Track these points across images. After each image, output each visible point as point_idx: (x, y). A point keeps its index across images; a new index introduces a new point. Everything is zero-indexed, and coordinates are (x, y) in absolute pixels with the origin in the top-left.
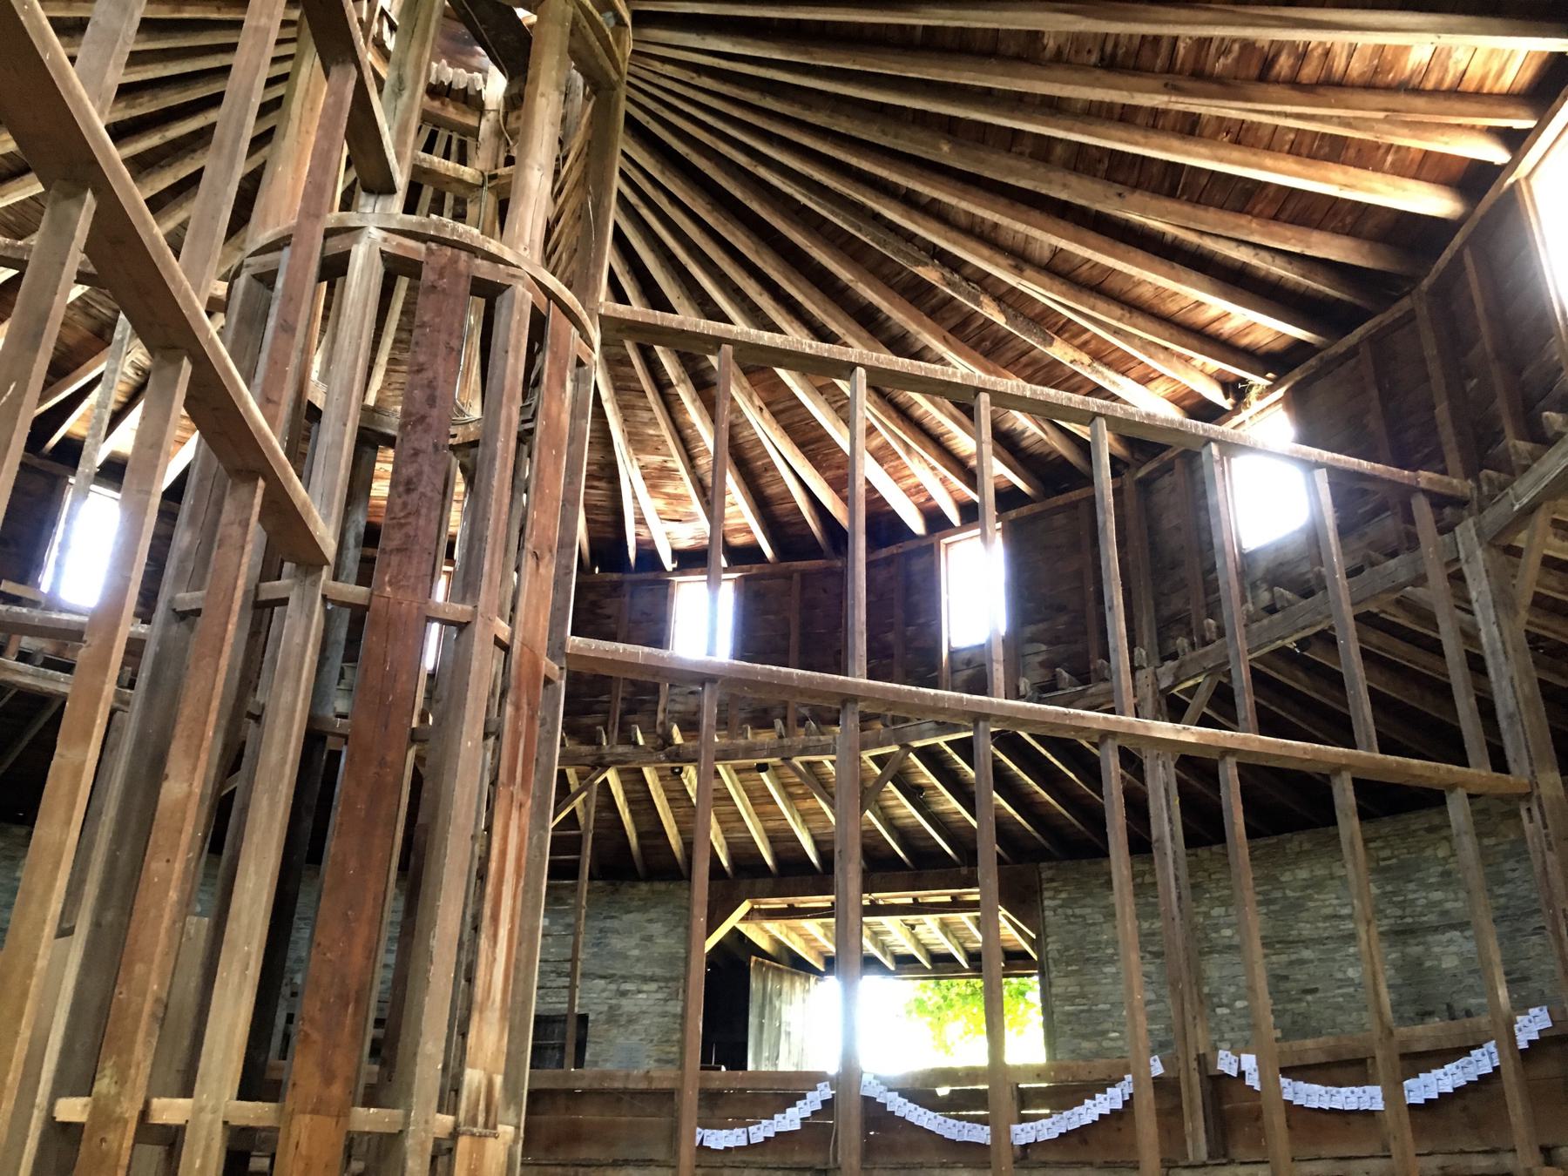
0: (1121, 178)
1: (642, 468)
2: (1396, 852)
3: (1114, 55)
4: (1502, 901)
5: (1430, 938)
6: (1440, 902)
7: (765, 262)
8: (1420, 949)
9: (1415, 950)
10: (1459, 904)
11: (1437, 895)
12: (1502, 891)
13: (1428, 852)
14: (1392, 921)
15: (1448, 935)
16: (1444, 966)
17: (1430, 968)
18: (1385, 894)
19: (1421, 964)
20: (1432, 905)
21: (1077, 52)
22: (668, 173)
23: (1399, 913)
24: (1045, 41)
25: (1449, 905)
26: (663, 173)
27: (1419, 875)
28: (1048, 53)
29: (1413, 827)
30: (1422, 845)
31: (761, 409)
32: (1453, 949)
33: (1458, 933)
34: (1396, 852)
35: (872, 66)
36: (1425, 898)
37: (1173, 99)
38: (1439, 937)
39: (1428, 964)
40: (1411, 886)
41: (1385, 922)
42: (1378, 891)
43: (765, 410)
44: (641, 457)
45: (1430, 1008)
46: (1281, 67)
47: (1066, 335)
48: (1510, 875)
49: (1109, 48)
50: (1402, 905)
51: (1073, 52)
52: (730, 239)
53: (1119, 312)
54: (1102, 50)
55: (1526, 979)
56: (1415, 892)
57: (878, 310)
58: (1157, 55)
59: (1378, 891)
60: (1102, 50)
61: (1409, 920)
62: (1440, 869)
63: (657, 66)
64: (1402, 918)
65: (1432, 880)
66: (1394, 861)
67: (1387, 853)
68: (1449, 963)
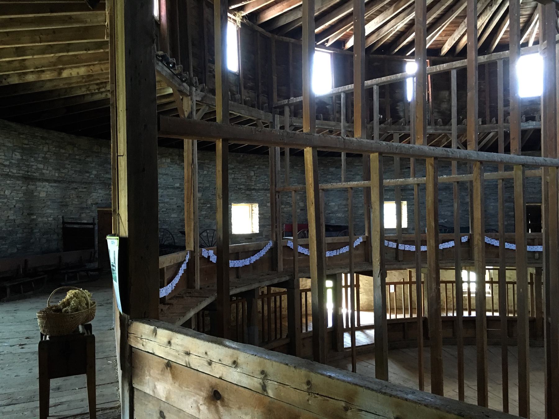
2: (30, 143)
4: (63, 175)
5: (38, 184)
6: (41, 169)
8: (33, 187)
9: (31, 187)
10: (48, 172)
11: (41, 166)
12: (64, 171)
13: (41, 147)
14: (23, 172)
15: (44, 183)
16: (41, 196)
17: (36, 196)
18: (22, 159)
19: (33, 193)
20: (38, 169)
23: (27, 169)
25: (44, 171)
27: (36, 155)
29: (37, 134)
30: (39, 143)
32: (44, 189)
33: (47, 184)
34: (30, 143)
36: (37, 166)
38: (41, 184)
39: (35, 194)
40: (32, 159)
41: (21, 172)
42: (20, 158)
45: (32, 212)
48: (67, 166)
50: (28, 166)
55: (67, 205)
56: (32, 162)
59: (20, 158)
61: (29, 174)
62: (44, 155)
64: (28, 172)
65: (40, 159)
66: (28, 146)
67: (26, 142)
68: (43, 195)
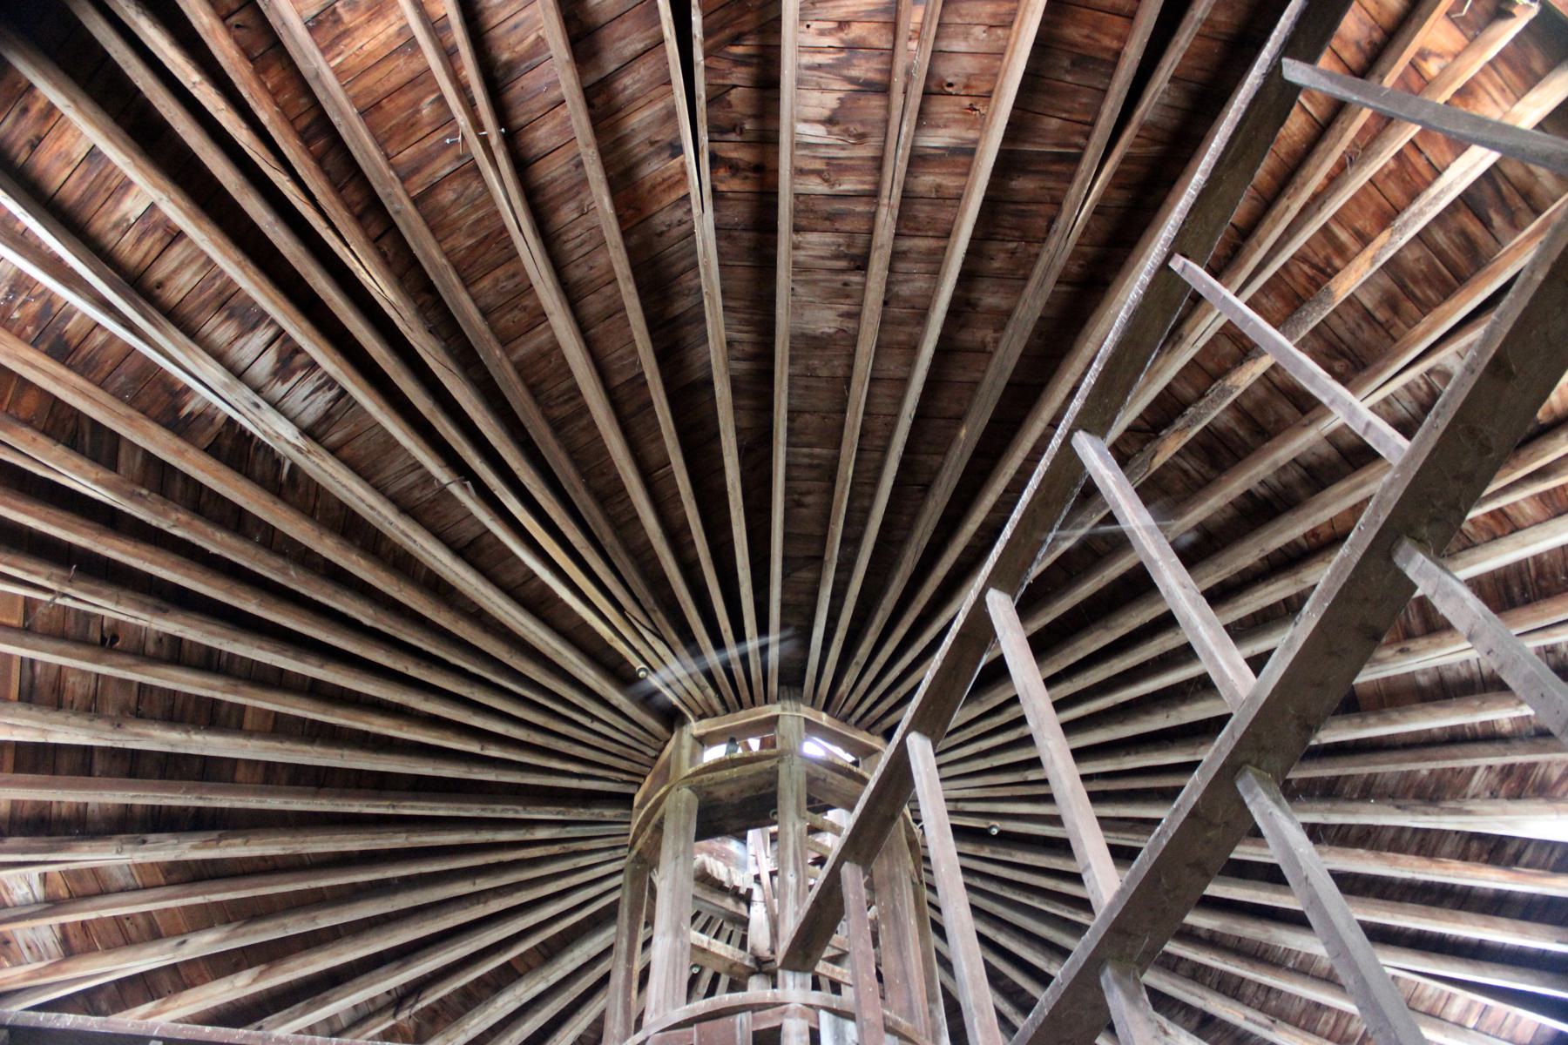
0: (1042, 223)
1: (1494, 795)
3: (852, 258)
7: (1122, 625)
21: (847, 296)
22: (983, 699)
24: (832, 331)
26: (981, 703)
28: (849, 325)
31: (1402, 651)
35: (839, 508)
37: (885, 201)
43: (1411, 645)
44: (1470, 792)
46: (867, 70)
47: (1337, 262)
49: (842, 264)
51: (848, 301)
52: (1080, 655)
53: (1284, 202)
54: (843, 271)
57: (1248, 494)
58: (851, 213)
60: (843, 271)
63: (844, 688)
